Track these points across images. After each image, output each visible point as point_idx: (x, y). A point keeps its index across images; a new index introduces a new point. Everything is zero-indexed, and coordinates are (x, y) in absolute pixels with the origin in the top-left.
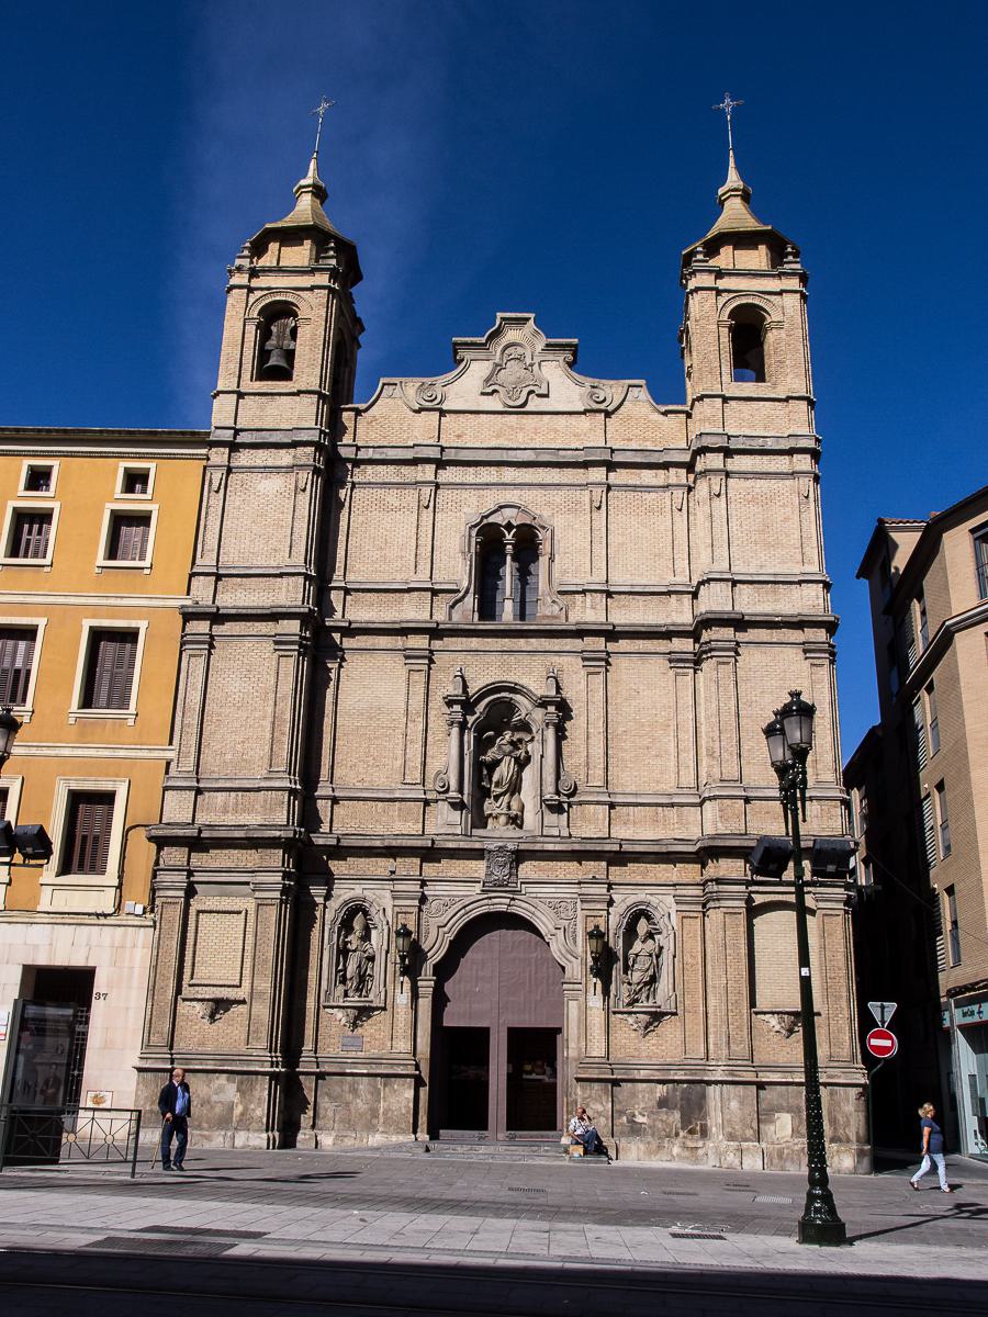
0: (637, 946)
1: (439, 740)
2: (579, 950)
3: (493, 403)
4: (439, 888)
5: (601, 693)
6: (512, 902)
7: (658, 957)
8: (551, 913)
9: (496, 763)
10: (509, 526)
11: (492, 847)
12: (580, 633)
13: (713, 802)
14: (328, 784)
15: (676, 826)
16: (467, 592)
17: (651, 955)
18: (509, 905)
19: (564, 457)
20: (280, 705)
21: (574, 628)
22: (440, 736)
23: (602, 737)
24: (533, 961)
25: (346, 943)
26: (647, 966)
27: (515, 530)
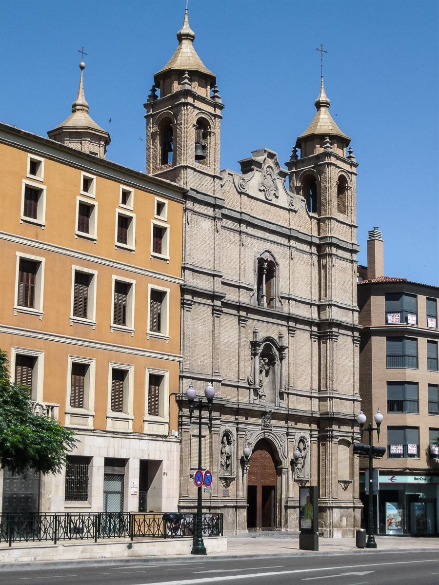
3: (261, 196)
4: (249, 427)
12: (288, 318)
19: (284, 231)
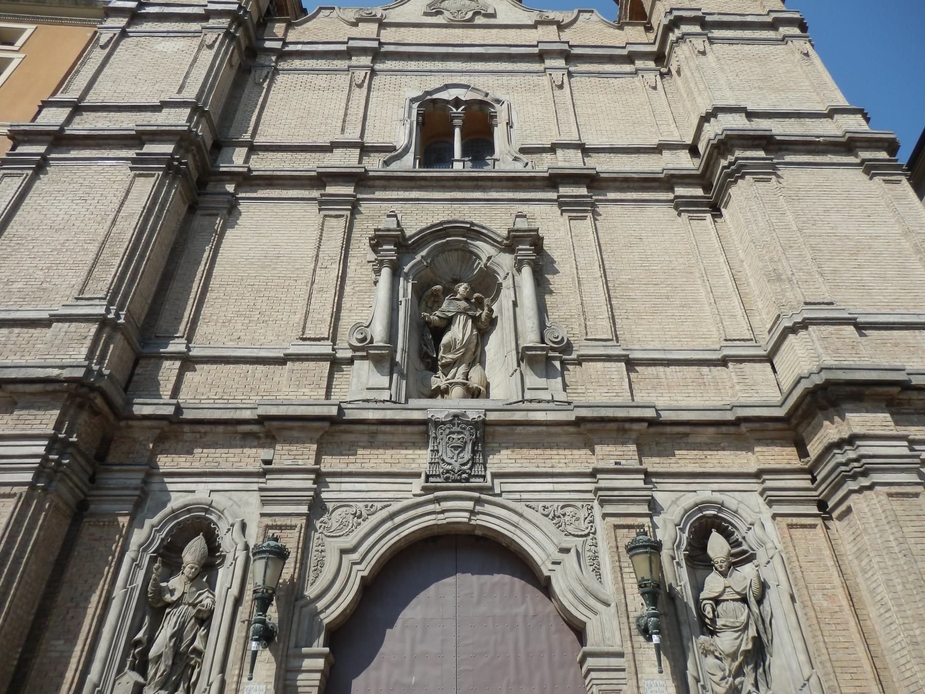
0: (714, 584)
1: (360, 291)
2: (609, 589)
5: (591, 237)
6: (478, 508)
7: (760, 602)
8: (548, 525)
9: (448, 322)
10: (457, 102)
11: (441, 416)
13: (802, 333)
14: (184, 341)
15: (737, 387)
16: (406, 150)
17: (744, 600)
18: (473, 512)
20: (120, 224)
21: (546, 175)
22: (364, 287)
23: (600, 283)
24: (520, 620)
25: (160, 592)
26: (743, 618)
27: (463, 107)
